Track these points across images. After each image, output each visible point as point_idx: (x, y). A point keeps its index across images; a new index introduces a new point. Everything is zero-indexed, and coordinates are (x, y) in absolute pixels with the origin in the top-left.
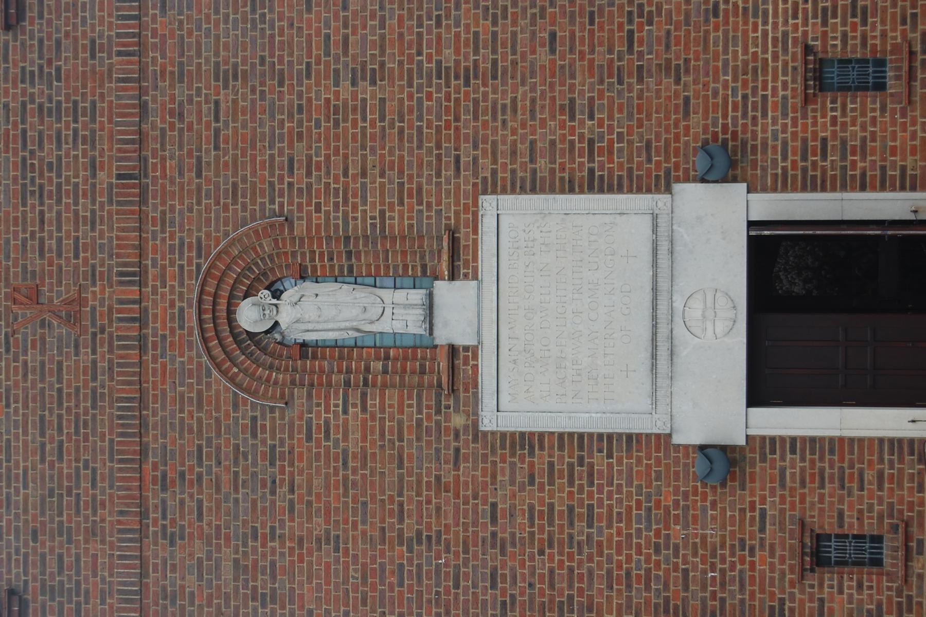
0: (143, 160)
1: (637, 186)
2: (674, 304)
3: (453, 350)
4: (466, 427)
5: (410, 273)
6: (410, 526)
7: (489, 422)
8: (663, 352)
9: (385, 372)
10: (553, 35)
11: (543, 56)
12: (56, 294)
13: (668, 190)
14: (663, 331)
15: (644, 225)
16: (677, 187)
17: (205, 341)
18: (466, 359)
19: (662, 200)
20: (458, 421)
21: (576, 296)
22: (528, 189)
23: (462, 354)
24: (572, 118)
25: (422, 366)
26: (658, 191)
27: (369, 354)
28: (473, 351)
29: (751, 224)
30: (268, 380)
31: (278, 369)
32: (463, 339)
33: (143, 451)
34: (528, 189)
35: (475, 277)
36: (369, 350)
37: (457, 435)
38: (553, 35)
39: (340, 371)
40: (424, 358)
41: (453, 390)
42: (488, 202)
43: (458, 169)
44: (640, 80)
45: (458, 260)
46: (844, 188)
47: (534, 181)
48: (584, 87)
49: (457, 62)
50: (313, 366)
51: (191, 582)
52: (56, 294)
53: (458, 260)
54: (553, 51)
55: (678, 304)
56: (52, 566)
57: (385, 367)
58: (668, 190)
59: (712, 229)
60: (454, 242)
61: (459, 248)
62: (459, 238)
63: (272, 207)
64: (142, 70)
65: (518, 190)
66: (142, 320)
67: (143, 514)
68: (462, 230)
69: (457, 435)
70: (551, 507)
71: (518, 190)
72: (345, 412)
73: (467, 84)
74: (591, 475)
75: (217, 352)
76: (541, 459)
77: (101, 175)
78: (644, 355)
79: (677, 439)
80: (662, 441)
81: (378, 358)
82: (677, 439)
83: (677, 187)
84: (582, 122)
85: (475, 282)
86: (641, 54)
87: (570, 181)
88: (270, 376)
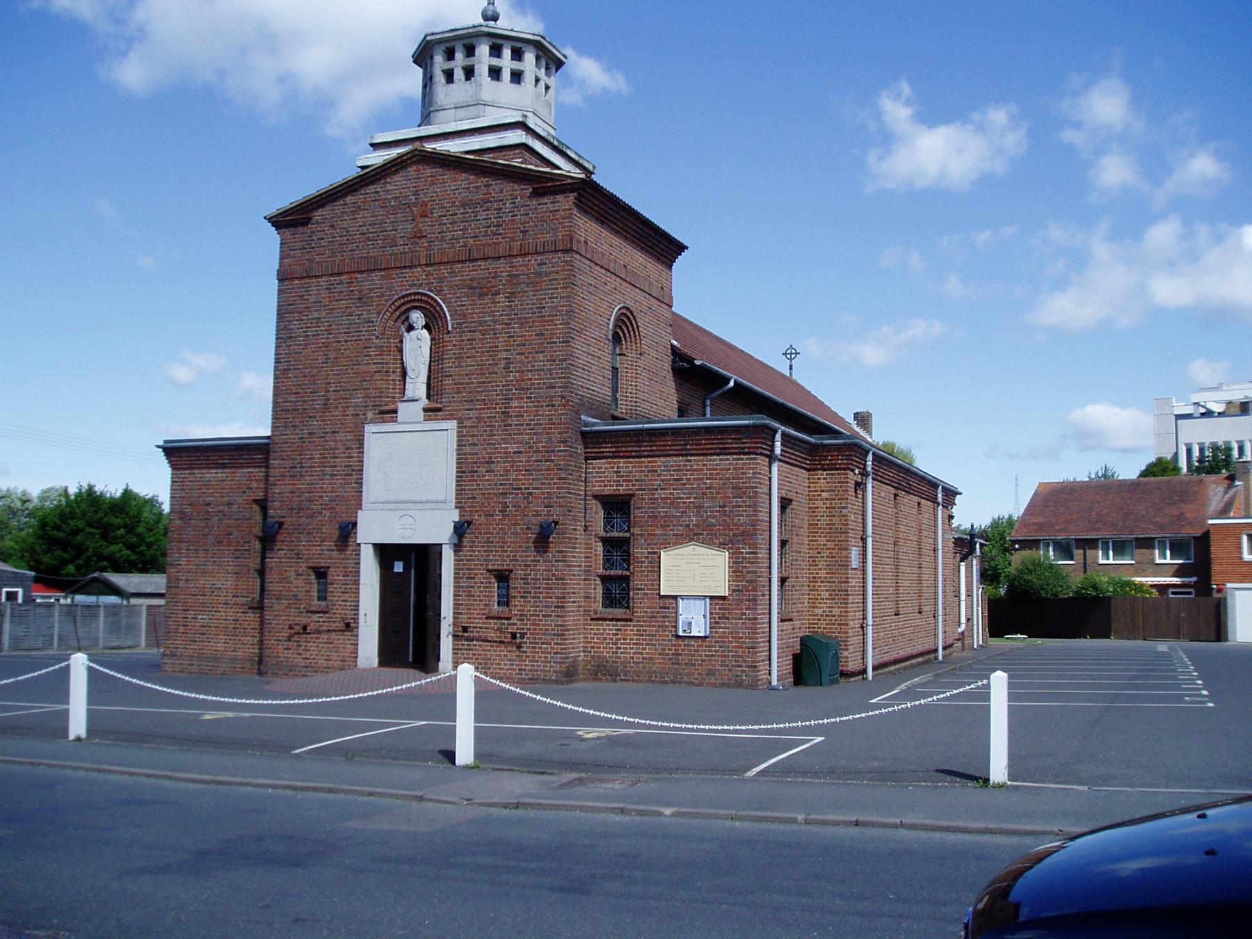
0: (476, 260)
3: (395, 412)
7: (369, 429)
8: (394, 506)
12: (424, 226)
14: (402, 506)
15: (441, 498)
16: (457, 511)
17: (403, 297)
19: (453, 506)
20: (370, 415)
28: (394, 420)
32: (401, 416)
33: (361, 272)
41: (382, 412)
42: (452, 425)
45: (431, 412)
51: (313, 299)
52: (424, 226)
53: (431, 412)
55: (409, 512)
56: (320, 235)
59: (434, 527)
60: (439, 410)
66: (411, 267)
67: (339, 274)
75: (397, 304)
76: (355, 453)
77: (471, 241)
78: (392, 498)
80: (359, 506)
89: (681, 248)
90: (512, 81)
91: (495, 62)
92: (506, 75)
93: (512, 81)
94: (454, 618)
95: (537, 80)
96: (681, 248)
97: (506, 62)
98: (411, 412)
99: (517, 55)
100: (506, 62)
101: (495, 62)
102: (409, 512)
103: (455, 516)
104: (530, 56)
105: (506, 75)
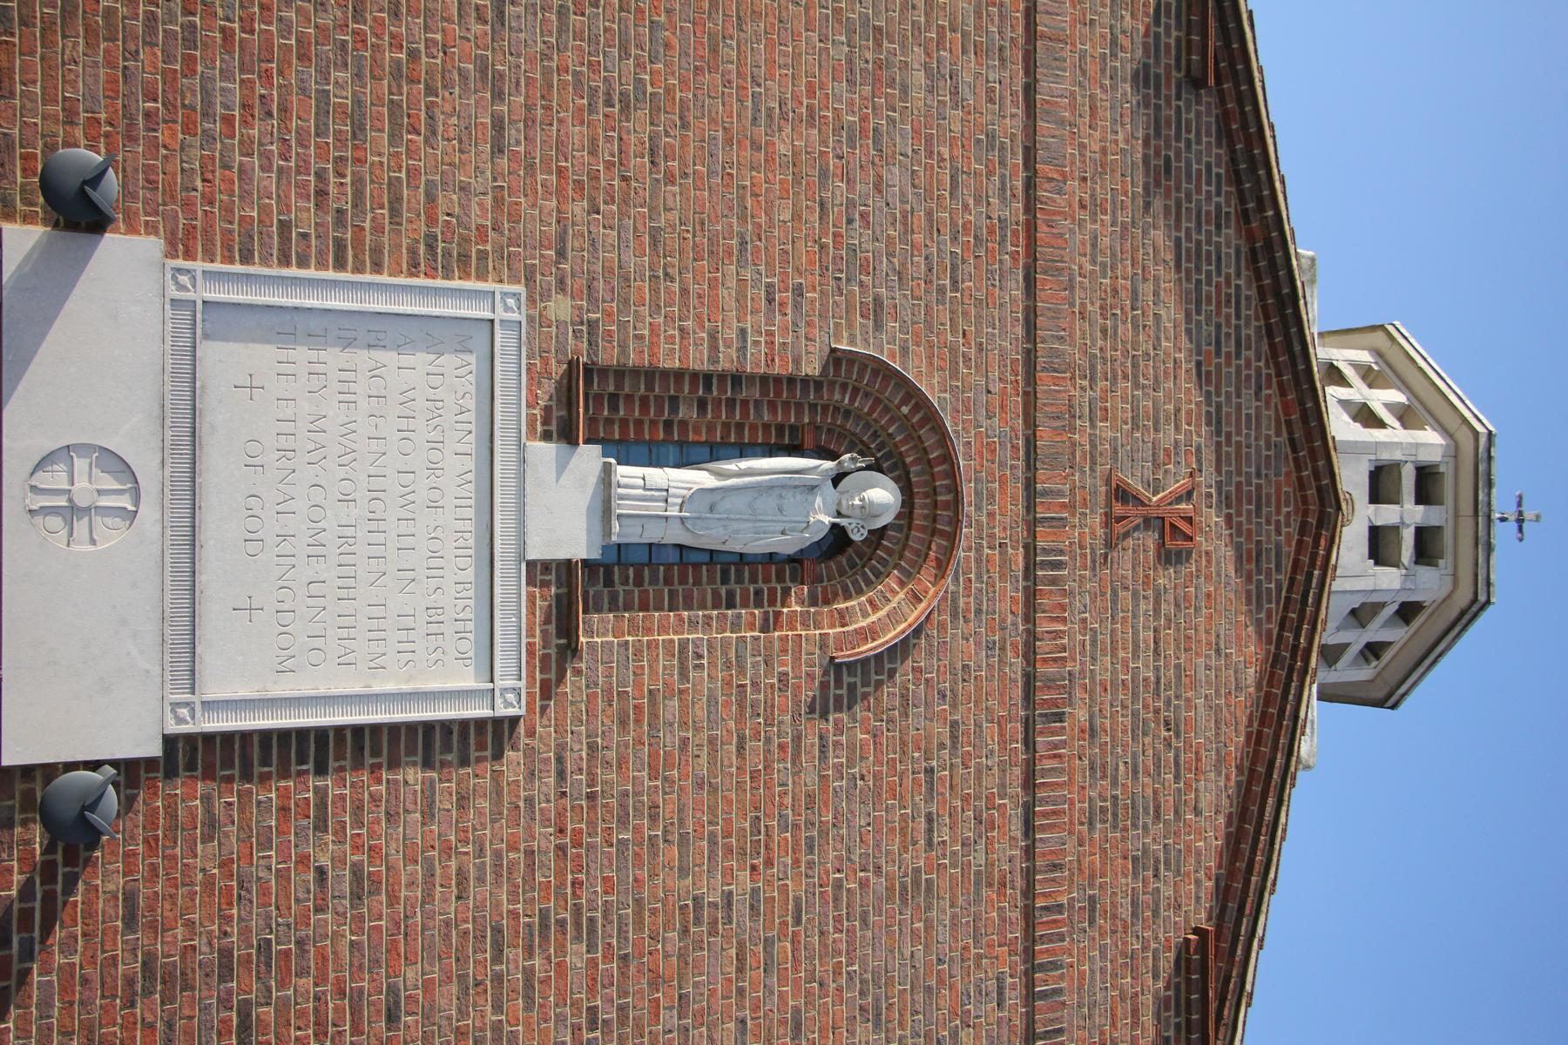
0: (1029, 743)
1: (232, 746)
2: (158, 516)
3: (567, 435)
4: (545, 296)
5: (631, 571)
6: (639, 127)
9: (674, 401)
10: (392, 1018)
13: (169, 741)
16: (154, 749)
18: (546, 422)
20: (560, 308)
21: (350, 531)
22: (438, 729)
23: (554, 428)
24: (357, 871)
25: (614, 408)
26: (190, 739)
27: (697, 431)
30: (856, 391)
31: (836, 409)
34: (438, 729)
35: (531, 565)
36: (696, 438)
37: (561, 283)
39: (745, 403)
40: (609, 422)
43: (560, 760)
44: (226, 953)
47: (428, 747)
48: (335, 927)
49: (561, 948)
50: (799, 415)
54: (393, 991)
57: (674, 408)
58: (169, 741)
61: (558, 619)
62: (559, 636)
63: (852, 680)
65: (456, 730)
68: (553, 651)
69: (561, 283)
70: (394, 138)
71: (456, 730)
72: (743, 332)
73: (544, 915)
74: (321, 193)
77: (1082, 715)
79: (152, 245)
80: (181, 244)
81: (683, 424)
82: (152, 245)
83: (154, 749)
84: (339, 861)
85: (531, 556)
86: (224, 1003)
87: (362, 749)
88: (852, 400)
98: (565, 502)
102: (149, 512)
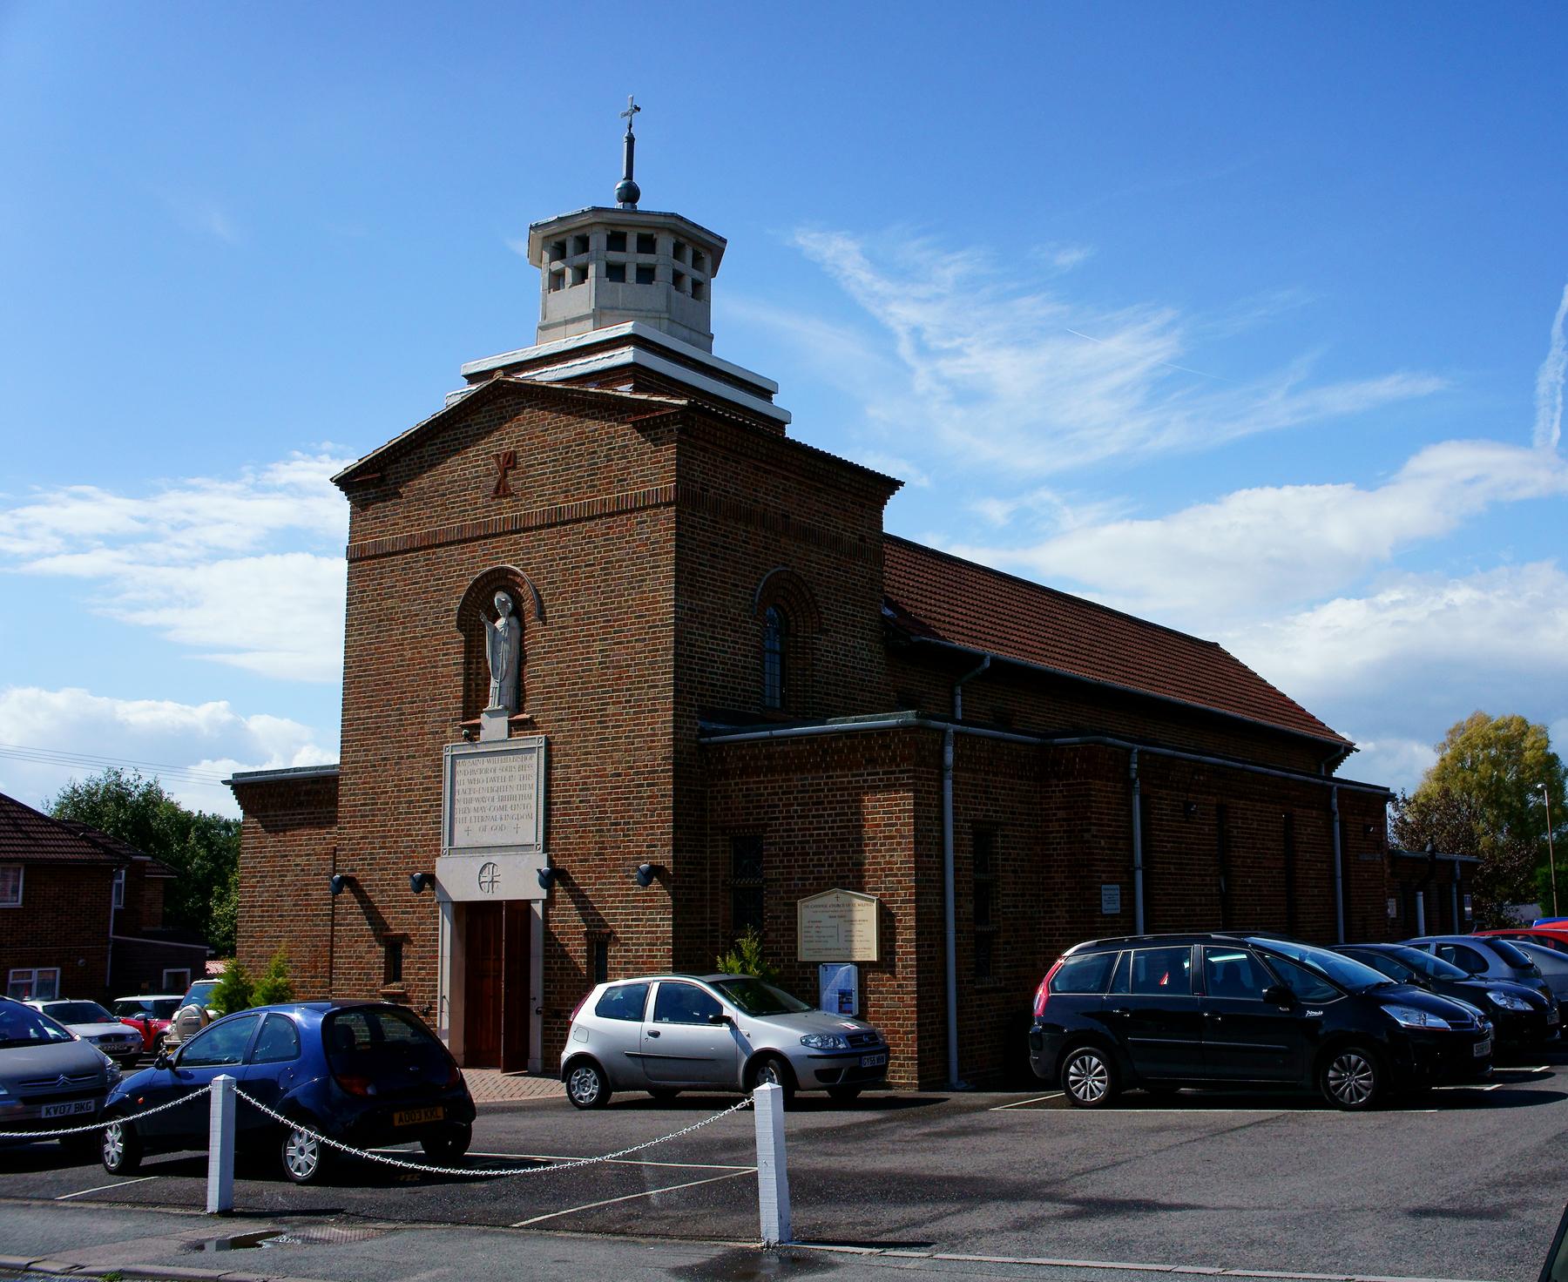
3: (478, 727)
7: (448, 751)
10: (619, 775)
11: (610, 769)
29: (528, 902)
38: (619, 775)
46: (545, 957)
59: (520, 880)
64: (611, 515)
89: (892, 485)
90: (638, 281)
91: (616, 257)
92: (631, 273)
93: (638, 281)
94: (545, 999)
95: (677, 278)
96: (892, 485)
97: (631, 258)
98: (494, 726)
99: (647, 244)
100: (631, 258)
101: (616, 257)
103: (542, 862)
104: (665, 243)
105: (631, 273)
